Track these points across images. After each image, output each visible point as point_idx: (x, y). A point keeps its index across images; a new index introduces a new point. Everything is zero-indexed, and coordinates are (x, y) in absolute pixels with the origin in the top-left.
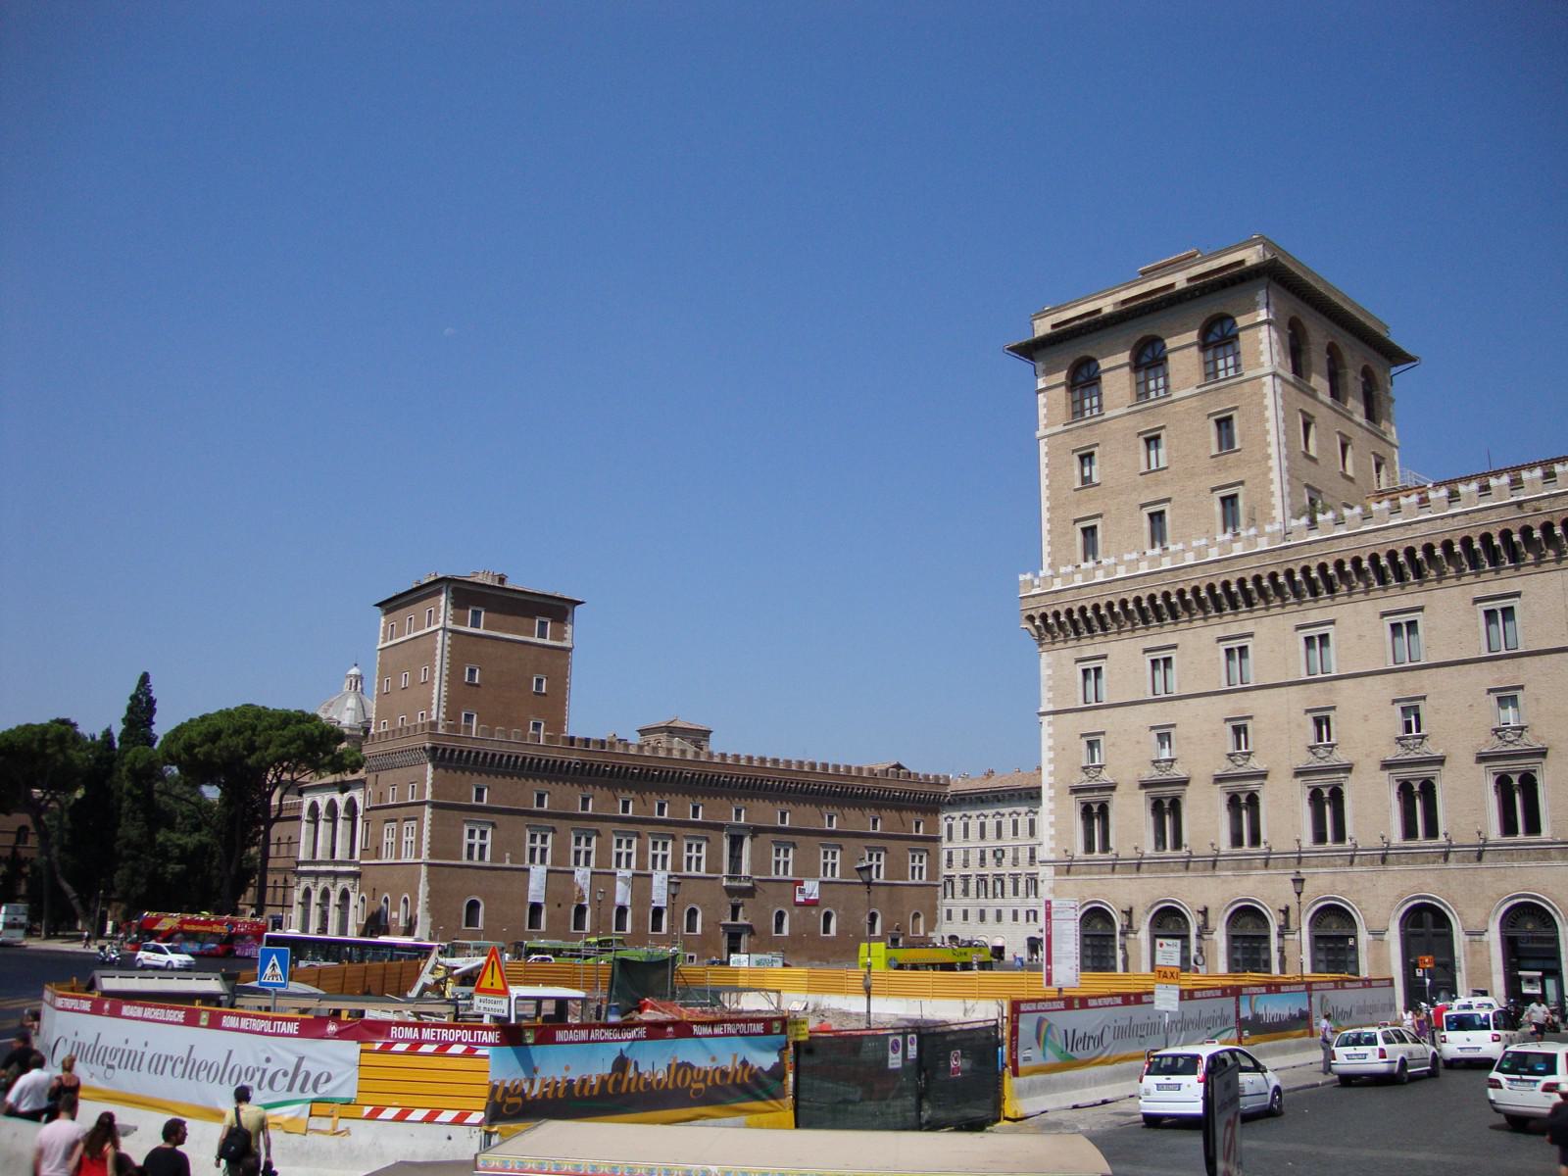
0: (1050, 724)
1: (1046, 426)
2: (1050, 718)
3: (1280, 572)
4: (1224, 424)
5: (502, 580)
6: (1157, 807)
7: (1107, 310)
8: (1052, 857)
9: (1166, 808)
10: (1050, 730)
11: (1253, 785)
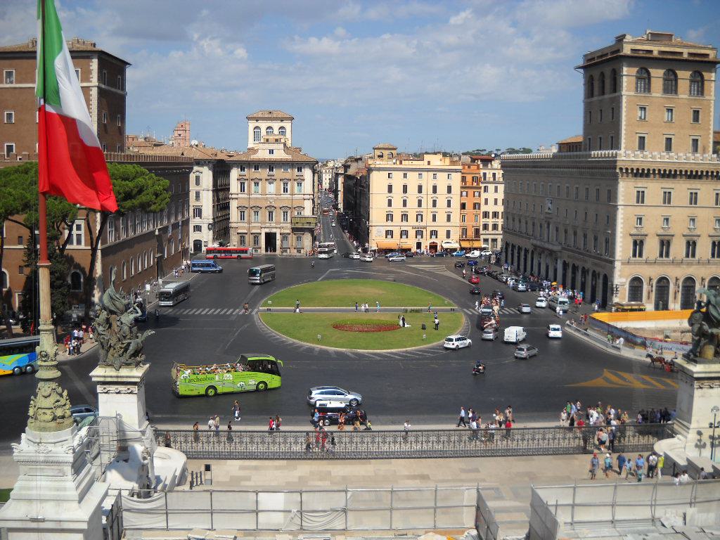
0: (622, 209)
1: (626, 91)
2: (623, 207)
3: (715, 171)
4: (696, 113)
5: (94, 45)
6: (662, 243)
7: (655, 54)
8: (620, 259)
9: (665, 244)
10: (622, 212)
11: (695, 238)
